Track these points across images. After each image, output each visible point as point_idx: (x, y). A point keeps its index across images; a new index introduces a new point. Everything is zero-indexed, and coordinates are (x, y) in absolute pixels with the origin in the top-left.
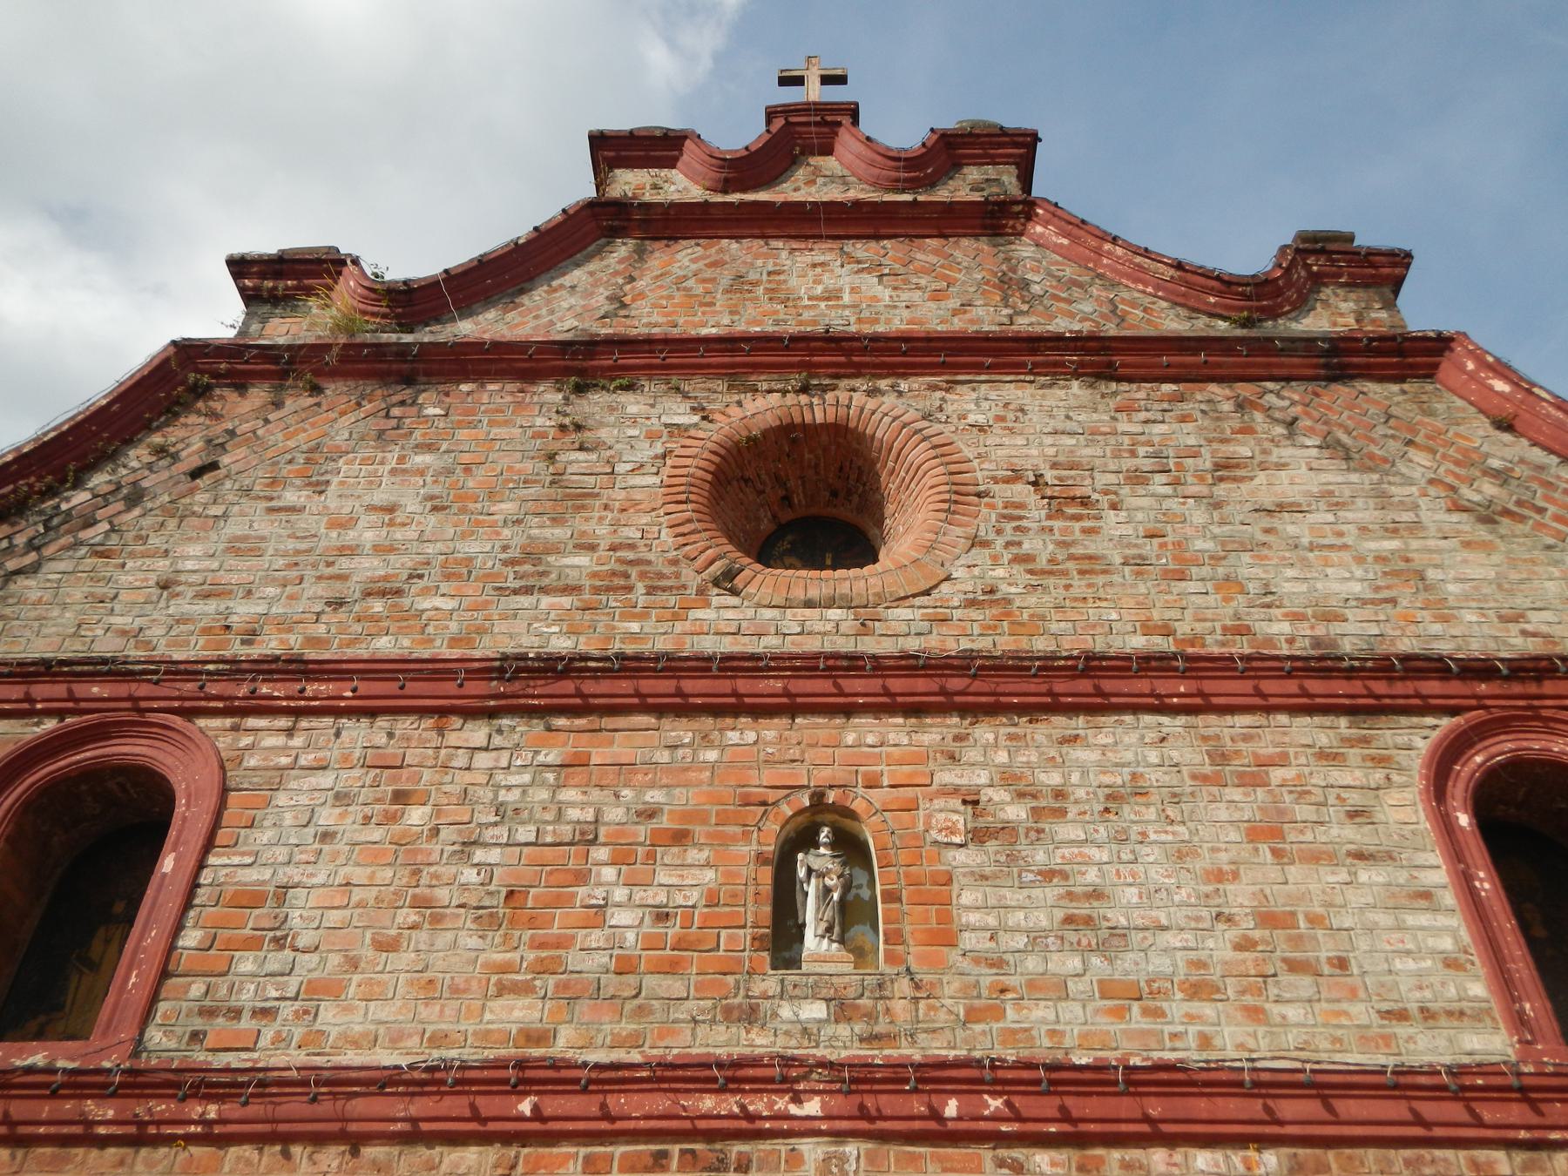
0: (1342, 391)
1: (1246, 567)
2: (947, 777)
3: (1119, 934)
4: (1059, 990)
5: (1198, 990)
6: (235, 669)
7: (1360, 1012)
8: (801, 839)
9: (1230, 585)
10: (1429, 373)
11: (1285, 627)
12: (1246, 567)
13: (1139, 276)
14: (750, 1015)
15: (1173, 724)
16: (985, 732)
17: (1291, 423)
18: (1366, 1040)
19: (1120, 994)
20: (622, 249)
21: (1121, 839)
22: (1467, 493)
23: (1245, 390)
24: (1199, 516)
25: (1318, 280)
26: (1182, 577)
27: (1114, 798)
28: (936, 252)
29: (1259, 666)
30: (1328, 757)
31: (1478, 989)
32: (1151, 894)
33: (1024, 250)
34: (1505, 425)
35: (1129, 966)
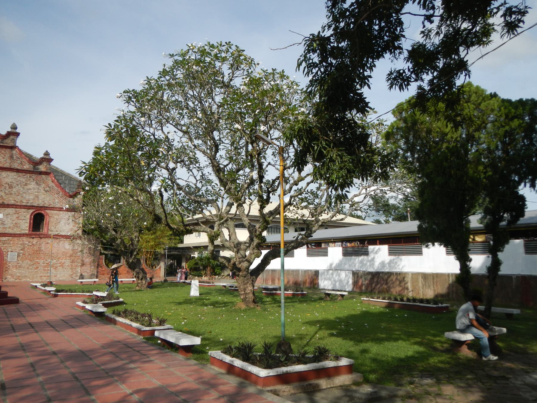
0: (40, 176)
1: (24, 195)
3: (5, 224)
5: (9, 228)
9: (22, 197)
10: (49, 175)
11: (25, 201)
12: (24, 195)
15: (13, 209)
17: (34, 180)
18: (20, 231)
19: (4, 228)
21: (7, 217)
22: (46, 189)
23: (31, 175)
24: (22, 190)
25: (43, 161)
27: (7, 215)
28: (5, 151)
30: (24, 212)
31: (28, 228)
32: (8, 222)
33: (14, 152)
34: (52, 182)
35: (5, 226)
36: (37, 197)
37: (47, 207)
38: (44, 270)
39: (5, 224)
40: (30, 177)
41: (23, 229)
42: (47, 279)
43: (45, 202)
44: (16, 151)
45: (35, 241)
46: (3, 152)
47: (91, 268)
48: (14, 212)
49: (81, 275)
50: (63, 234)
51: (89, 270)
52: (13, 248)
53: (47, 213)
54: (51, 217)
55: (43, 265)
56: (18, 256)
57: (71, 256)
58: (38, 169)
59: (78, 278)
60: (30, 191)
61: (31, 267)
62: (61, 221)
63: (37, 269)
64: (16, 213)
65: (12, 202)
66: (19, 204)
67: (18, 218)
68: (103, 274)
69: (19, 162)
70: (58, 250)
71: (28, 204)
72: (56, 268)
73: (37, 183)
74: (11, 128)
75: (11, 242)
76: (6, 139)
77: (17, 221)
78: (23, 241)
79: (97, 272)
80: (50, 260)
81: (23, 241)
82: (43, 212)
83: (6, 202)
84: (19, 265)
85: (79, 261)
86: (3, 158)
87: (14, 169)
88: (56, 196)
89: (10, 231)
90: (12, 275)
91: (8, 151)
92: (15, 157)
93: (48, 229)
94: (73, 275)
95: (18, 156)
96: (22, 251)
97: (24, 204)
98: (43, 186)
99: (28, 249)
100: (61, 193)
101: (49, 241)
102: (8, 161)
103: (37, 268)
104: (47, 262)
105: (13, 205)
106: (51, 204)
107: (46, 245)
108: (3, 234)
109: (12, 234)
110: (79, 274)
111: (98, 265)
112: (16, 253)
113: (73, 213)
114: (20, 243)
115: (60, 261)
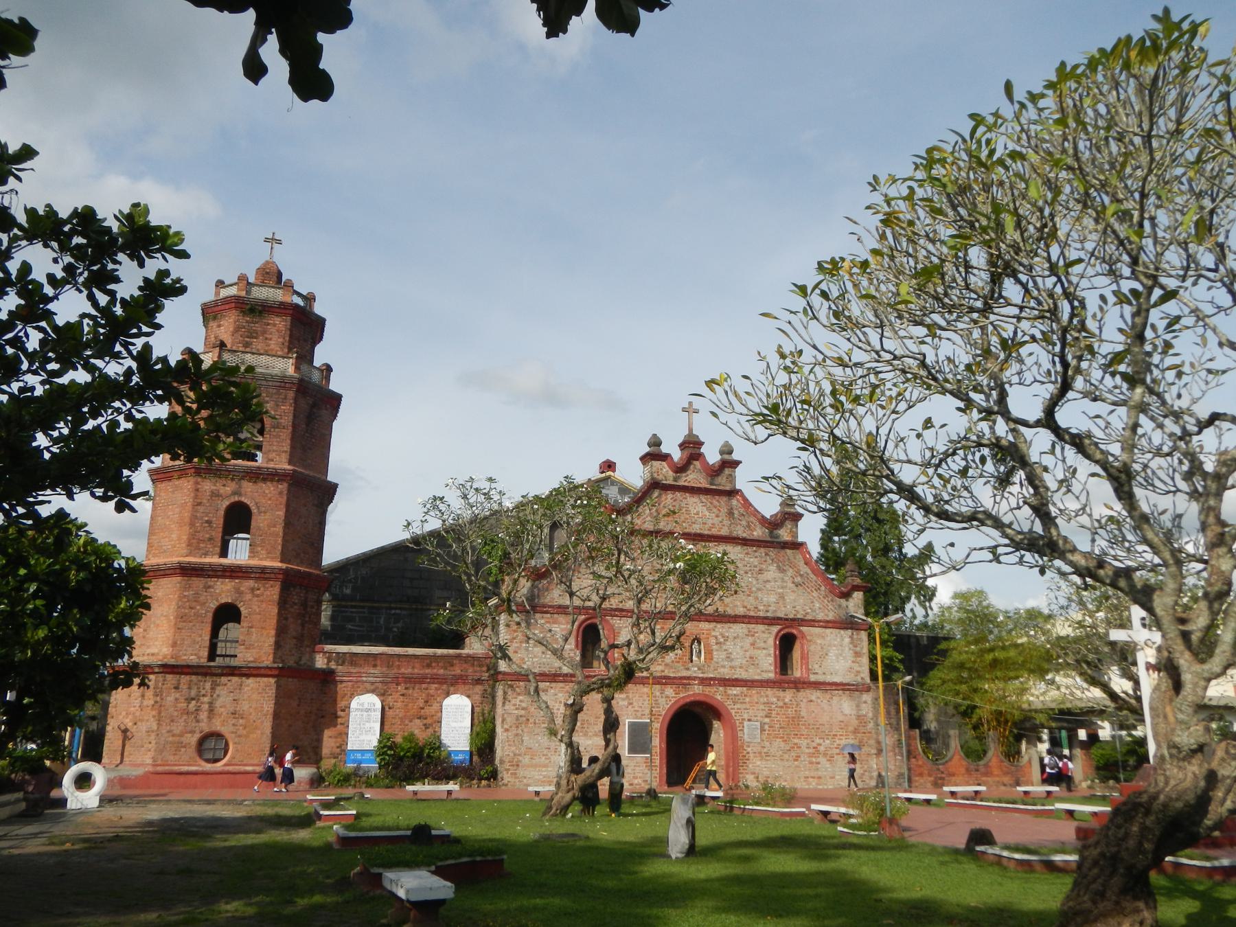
0: (782, 552)
2: (713, 634)
4: (723, 667)
5: (741, 667)
6: (612, 610)
7: (759, 671)
8: (694, 640)
9: (757, 598)
10: (798, 549)
13: (755, 516)
14: (688, 669)
15: (744, 625)
16: (719, 626)
20: (656, 493)
23: (767, 550)
24: (754, 582)
25: (786, 519)
26: (749, 595)
29: (758, 618)
32: (738, 653)
33: (734, 502)
34: (806, 564)
35: (733, 664)
36: (782, 597)
37: (802, 620)
38: (811, 763)
39: (732, 660)
40: (767, 554)
41: (764, 669)
42: (818, 784)
43: (798, 608)
44: (738, 500)
45: (788, 695)
46: (715, 502)
47: (896, 760)
48: (746, 631)
49: (880, 775)
50: (837, 679)
51: (893, 765)
52: (751, 711)
53: (800, 631)
54: (810, 641)
55: (807, 751)
56: (762, 730)
57: (856, 731)
58: (778, 537)
59: (873, 783)
60: (768, 586)
61: (786, 756)
62: (829, 651)
63: (797, 760)
64: (750, 634)
65: (740, 611)
66: (752, 614)
67: (753, 644)
68: (921, 775)
69: (744, 523)
70: (831, 718)
71: (769, 614)
72: (831, 759)
73: (778, 567)
74: (722, 453)
75: (747, 699)
76: (718, 475)
77: (752, 652)
78: (767, 696)
79: (909, 769)
80: (818, 741)
81: (767, 696)
82: (795, 632)
83: (730, 611)
84: (765, 750)
85: (872, 742)
86: (717, 516)
87: (739, 538)
88: (815, 594)
89: (743, 673)
90: (754, 773)
91: (724, 499)
92: (736, 512)
93: (808, 669)
94: (863, 774)
95: (742, 510)
96: (767, 720)
97: (761, 614)
98: (790, 572)
99: (778, 714)
100: (823, 588)
101: (814, 695)
102: (725, 522)
103: (797, 758)
104: (814, 745)
105: (744, 617)
106: (807, 613)
107: (813, 705)
108: (733, 680)
109: (749, 681)
110: (875, 774)
111: (909, 753)
112: (758, 724)
113: (849, 632)
114: (762, 700)
115: (838, 742)
